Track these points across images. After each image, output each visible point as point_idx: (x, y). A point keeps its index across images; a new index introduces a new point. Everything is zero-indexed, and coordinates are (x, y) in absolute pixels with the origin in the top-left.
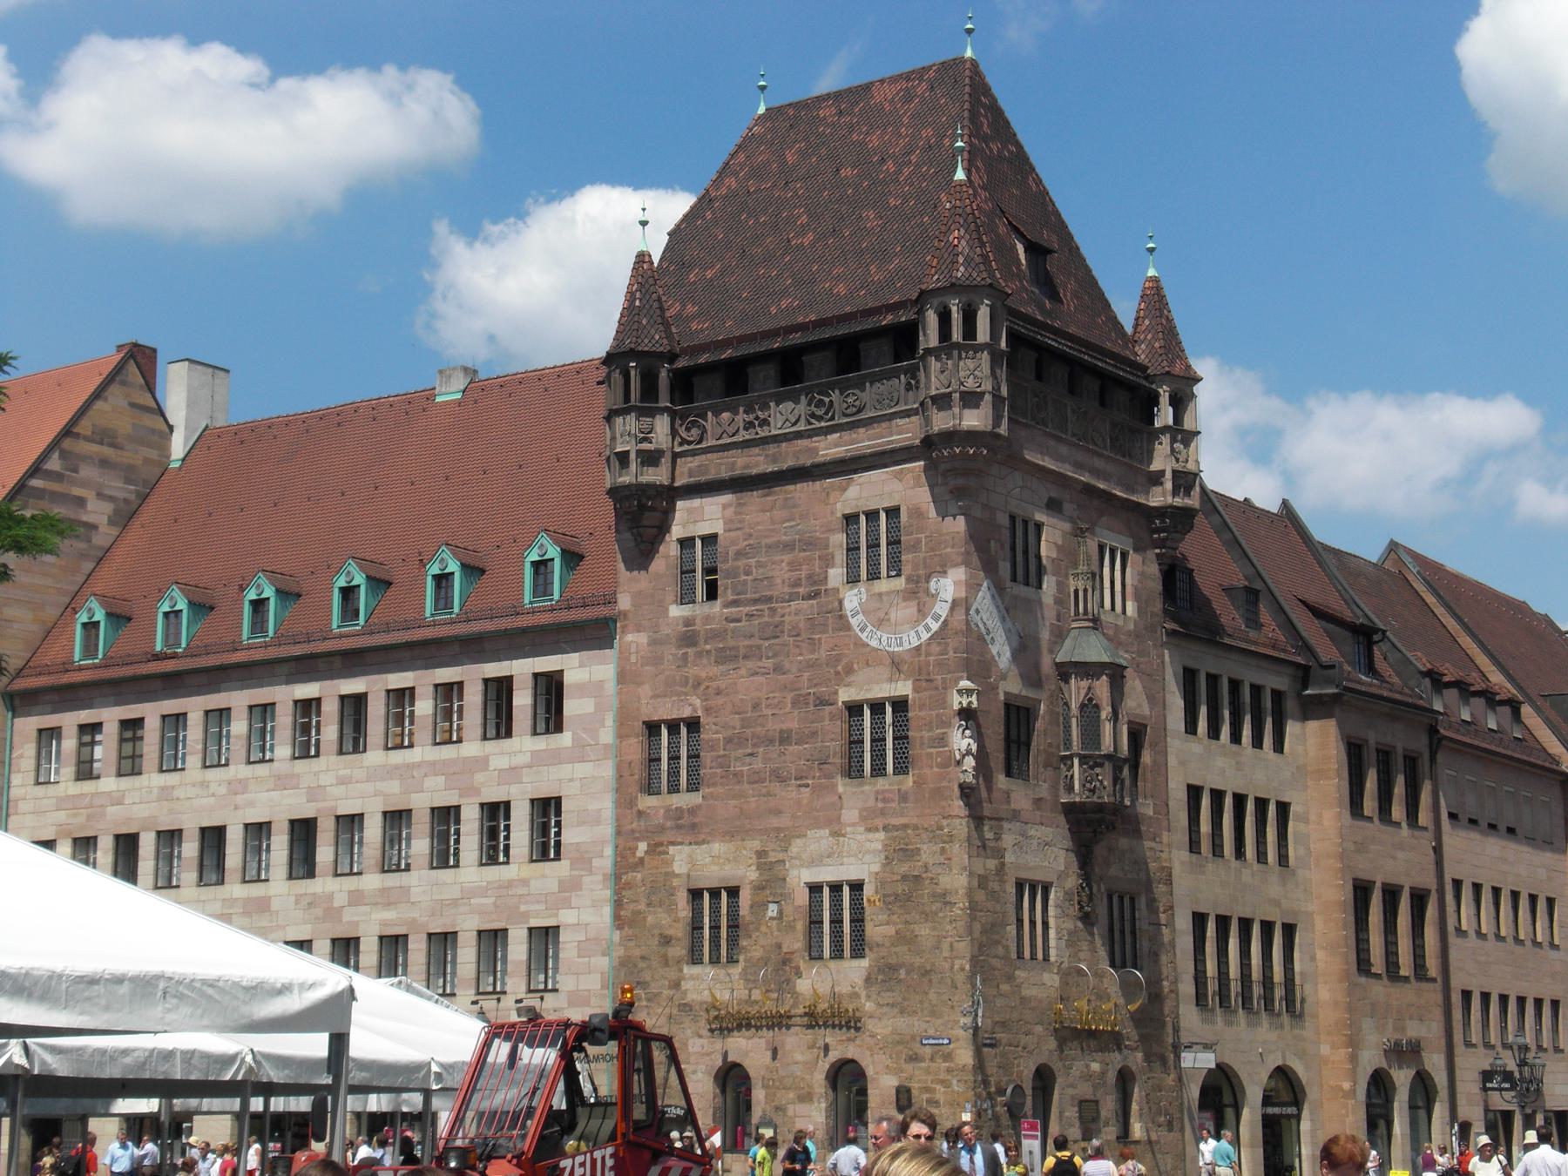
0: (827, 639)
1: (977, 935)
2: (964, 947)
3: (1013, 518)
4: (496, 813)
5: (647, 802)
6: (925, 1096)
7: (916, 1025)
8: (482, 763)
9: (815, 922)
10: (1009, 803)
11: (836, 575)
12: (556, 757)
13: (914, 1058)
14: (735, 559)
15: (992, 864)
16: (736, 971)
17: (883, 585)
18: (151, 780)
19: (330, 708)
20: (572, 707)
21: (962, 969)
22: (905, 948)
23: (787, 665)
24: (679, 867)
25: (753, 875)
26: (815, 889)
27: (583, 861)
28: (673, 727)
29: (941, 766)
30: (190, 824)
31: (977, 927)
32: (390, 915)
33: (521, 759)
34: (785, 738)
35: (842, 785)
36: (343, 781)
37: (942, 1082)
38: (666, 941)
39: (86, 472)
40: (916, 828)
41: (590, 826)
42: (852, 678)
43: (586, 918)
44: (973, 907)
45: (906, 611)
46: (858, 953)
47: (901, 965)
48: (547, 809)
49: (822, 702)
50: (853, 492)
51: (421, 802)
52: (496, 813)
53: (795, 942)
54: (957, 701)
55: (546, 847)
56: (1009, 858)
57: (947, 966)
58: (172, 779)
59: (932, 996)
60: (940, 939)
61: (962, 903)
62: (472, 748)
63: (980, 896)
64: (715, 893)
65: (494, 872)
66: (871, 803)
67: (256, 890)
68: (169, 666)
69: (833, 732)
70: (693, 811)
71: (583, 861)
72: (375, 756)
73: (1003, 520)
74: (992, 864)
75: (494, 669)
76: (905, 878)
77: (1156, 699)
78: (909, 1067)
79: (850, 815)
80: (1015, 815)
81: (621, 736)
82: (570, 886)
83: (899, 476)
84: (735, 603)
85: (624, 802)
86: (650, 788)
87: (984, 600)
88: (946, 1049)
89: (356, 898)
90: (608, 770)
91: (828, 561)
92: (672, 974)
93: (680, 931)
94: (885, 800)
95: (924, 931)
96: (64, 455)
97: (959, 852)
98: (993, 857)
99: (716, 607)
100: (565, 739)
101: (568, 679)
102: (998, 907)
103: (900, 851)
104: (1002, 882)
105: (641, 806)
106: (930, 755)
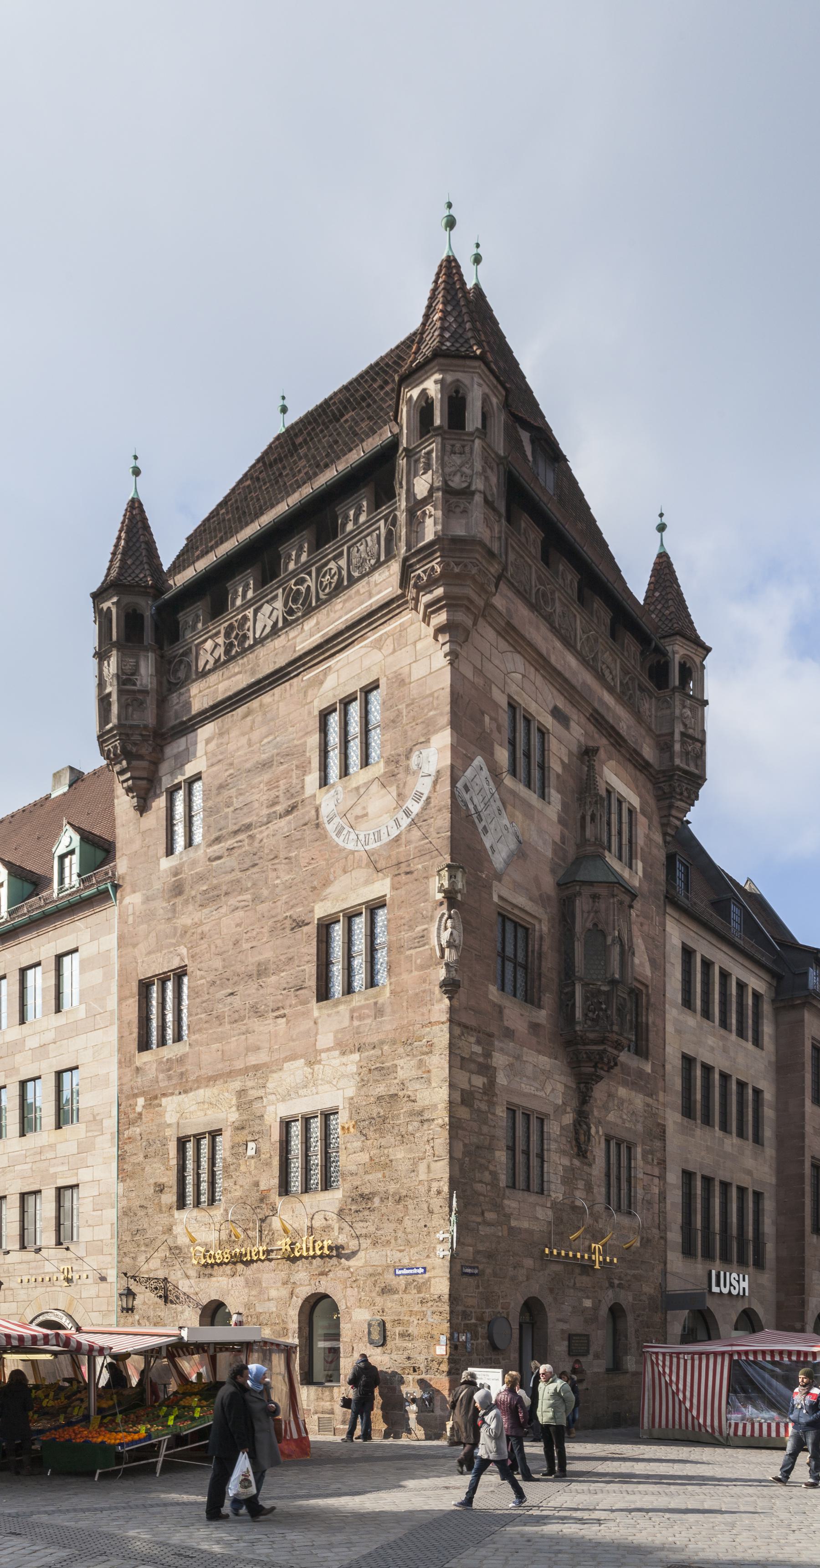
0: (304, 855)
1: (459, 1155)
2: (442, 1169)
6: (398, 1329)
7: (393, 1255)
10: (501, 1018)
13: (386, 1290)
14: (218, 794)
15: (479, 1081)
21: (439, 1192)
22: (380, 1175)
23: (265, 892)
29: (422, 967)
35: (316, 1009)
37: (416, 1313)
40: (394, 1042)
42: (328, 890)
44: (455, 1127)
46: (327, 1184)
47: (374, 1194)
49: (299, 924)
56: (501, 1079)
57: (423, 1189)
59: (407, 1222)
60: (415, 1162)
61: (442, 1116)
63: (464, 1113)
66: (346, 1022)
76: (380, 1098)
78: (379, 1300)
80: (509, 1034)
84: (218, 840)
88: (420, 1279)
90: (112, 1035)
92: (163, 1219)
94: (360, 1018)
95: (399, 1154)
97: (439, 1064)
98: (479, 1073)
102: (485, 1129)
104: (491, 1104)
105: (138, 1064)
106: (409, 958)
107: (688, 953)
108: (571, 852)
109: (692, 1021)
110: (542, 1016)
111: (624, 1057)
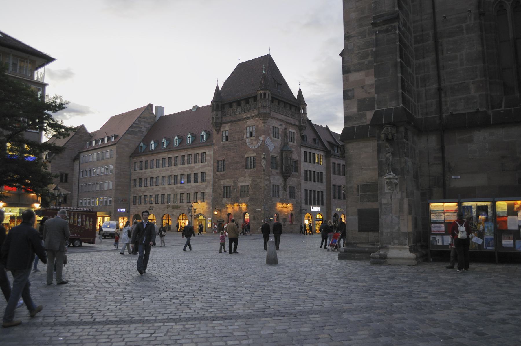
3: (273, 127)
4: (196, 174)
5: (218, 173)
8: (194, 167)
9: (241, 192)
11: (245, 136)
12: (205, 166)
16: (230, 199)
17: (252, 138)
18: (149, 170)
19: (173, 158)
20: (207, 158)
24: (222, 183)
25: (233, 184)
26: (241, 186)
27: (208, 182)
28: (221, 161)
30: (155, 176)
31: (265, 192)
32: (182, 190)
33: (200, 166)
34: (237, 163)
35: (245, 170)
36: (175, 170)
38: (220, 194)
39: (142, 123)
41: (209, 177)
43: (209, 190)
45: (254, 142)
48: (203, 174)
49: (243, 157)
50: (248, 123)
51: (186, 173)
52: (196, 174)
53: (238, 195)
54: (263, 156)
55: (203, 180)
56: (272, 181)
58: (152, 170)
62: (193, 165)
63: (266, 187)
64: (227, 187)
65: (196, 184)
67: (163, 186)
68: (152, 153)
69: (245, 161)
70: (224, 174)
71: (208, 182)
72: (179, 166)
73: (271, 127)
74: (268, 182)
75: (196, 152)
77: (300, 156)
79: (247, 175)
80: (273, 174)
81: (214, 163)
82: (207, 186)
83: (254, 120)
85: (214, 173)
86: (218, 171)
87: (268, 139)
89: (177, 188)
91: (244, 134)
93: (222, 193)
95: (257, 193)
96: (138, 121)
99: (228, 142)
100: (206, 163)
101: (207, 153)
103: (254, 180)
107: (306, 152)
108: (283, 144)
109: (306, 164)
110: (278, 171)
111: (293, 173)
